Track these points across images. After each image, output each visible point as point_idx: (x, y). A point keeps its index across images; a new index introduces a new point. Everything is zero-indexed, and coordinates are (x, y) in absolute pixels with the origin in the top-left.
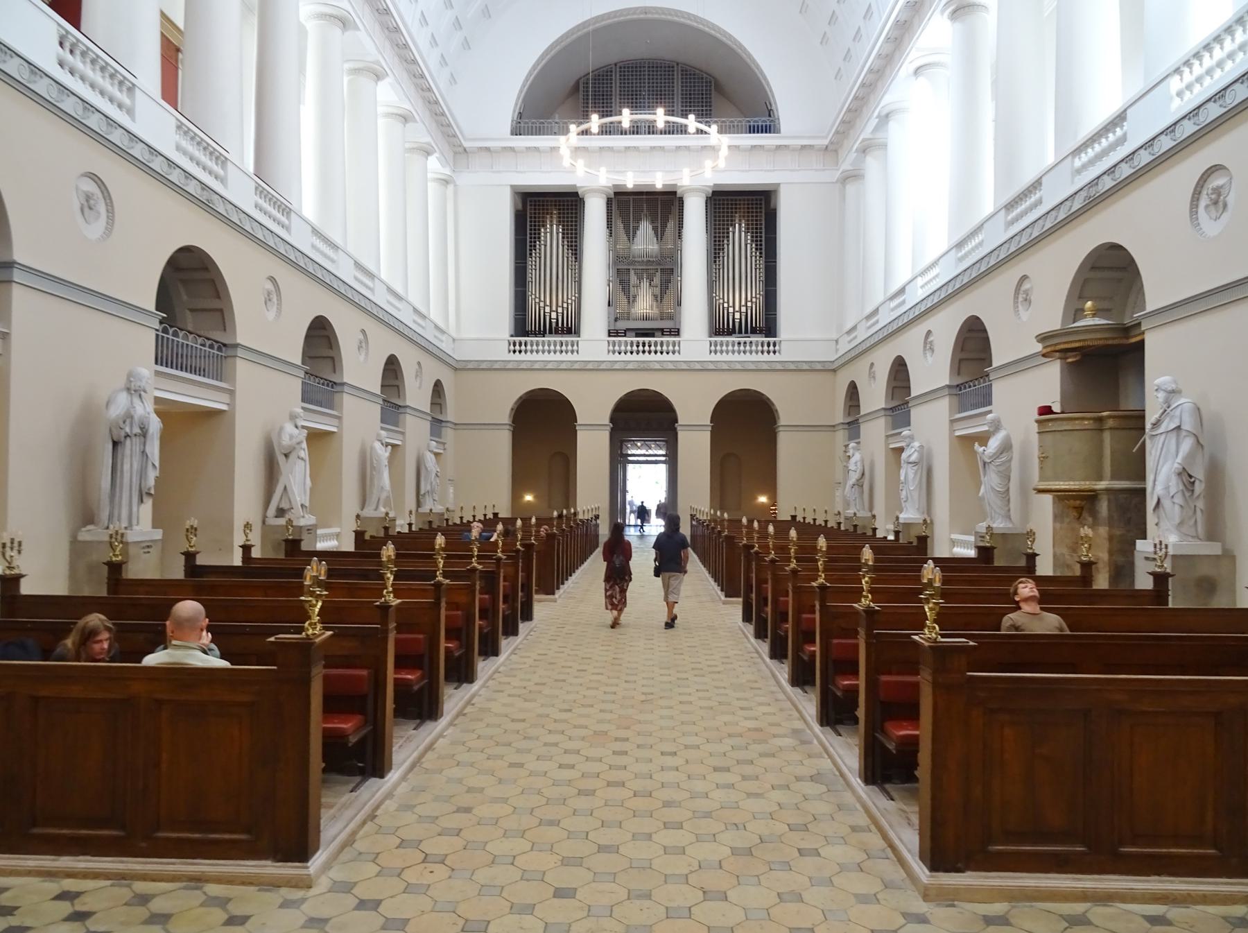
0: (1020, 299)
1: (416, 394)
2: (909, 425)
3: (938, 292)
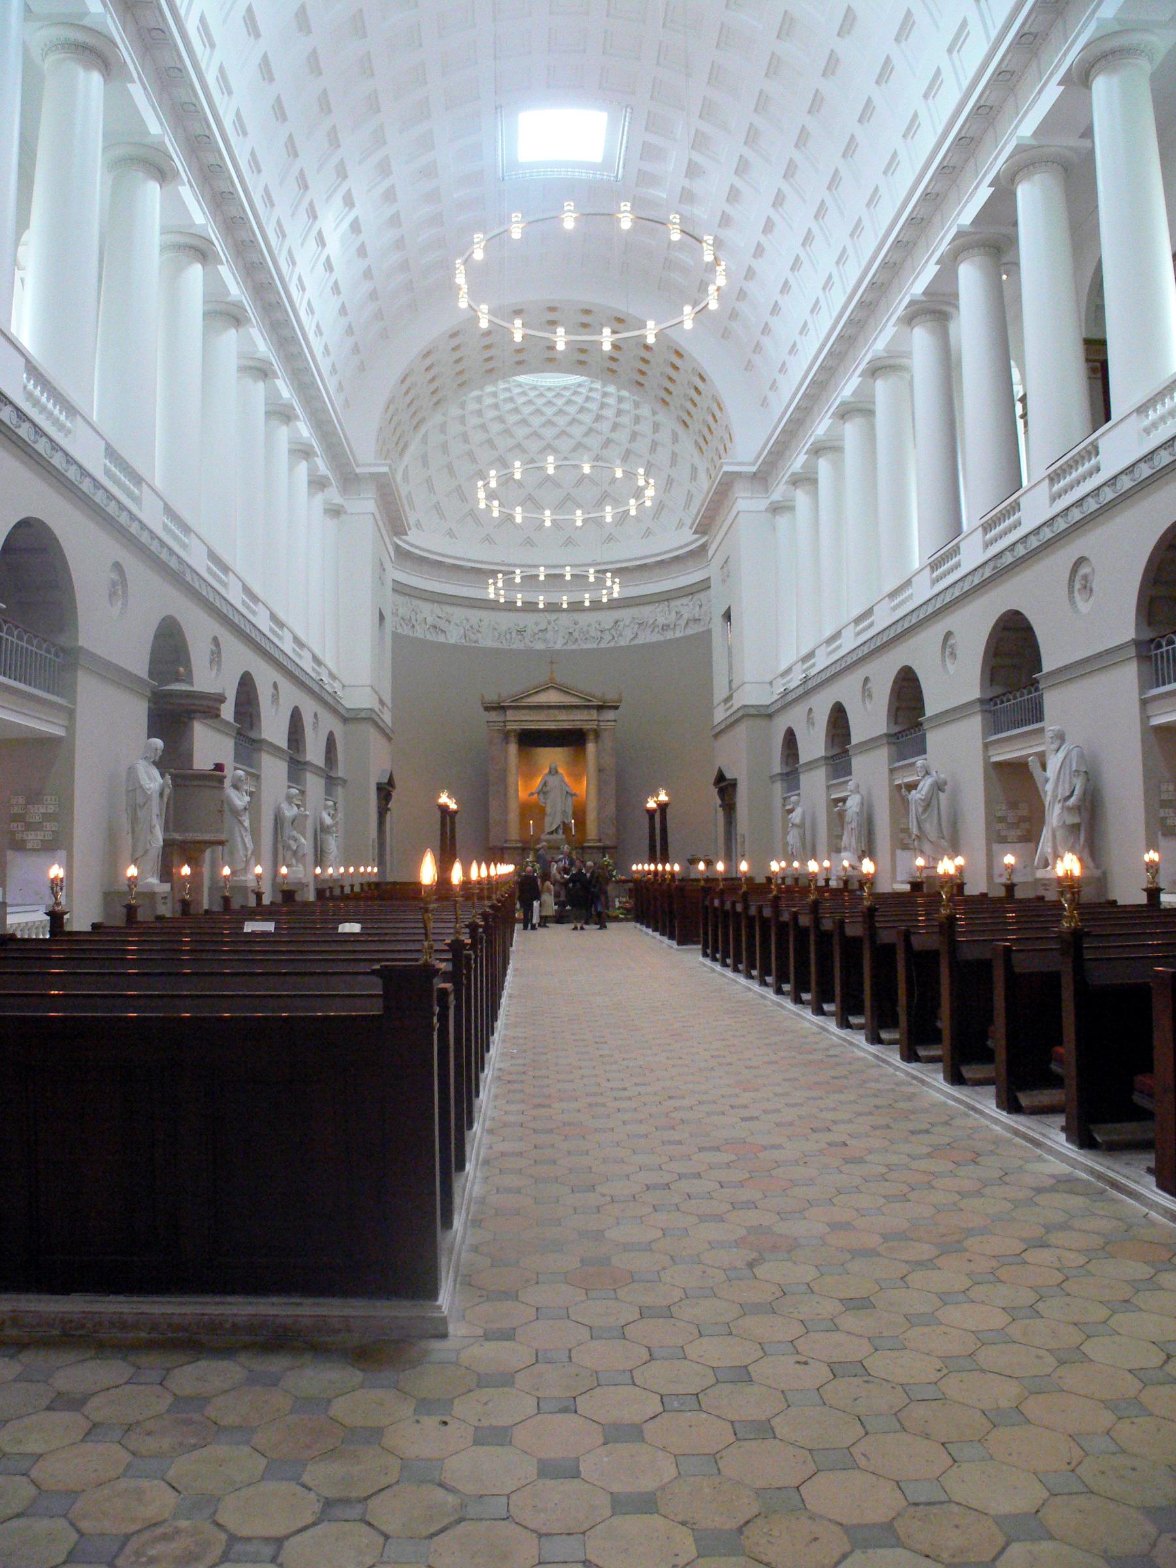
0: (1077, 586)
1: (273, 728)
2: (925, 752)
3: (960, 584)
